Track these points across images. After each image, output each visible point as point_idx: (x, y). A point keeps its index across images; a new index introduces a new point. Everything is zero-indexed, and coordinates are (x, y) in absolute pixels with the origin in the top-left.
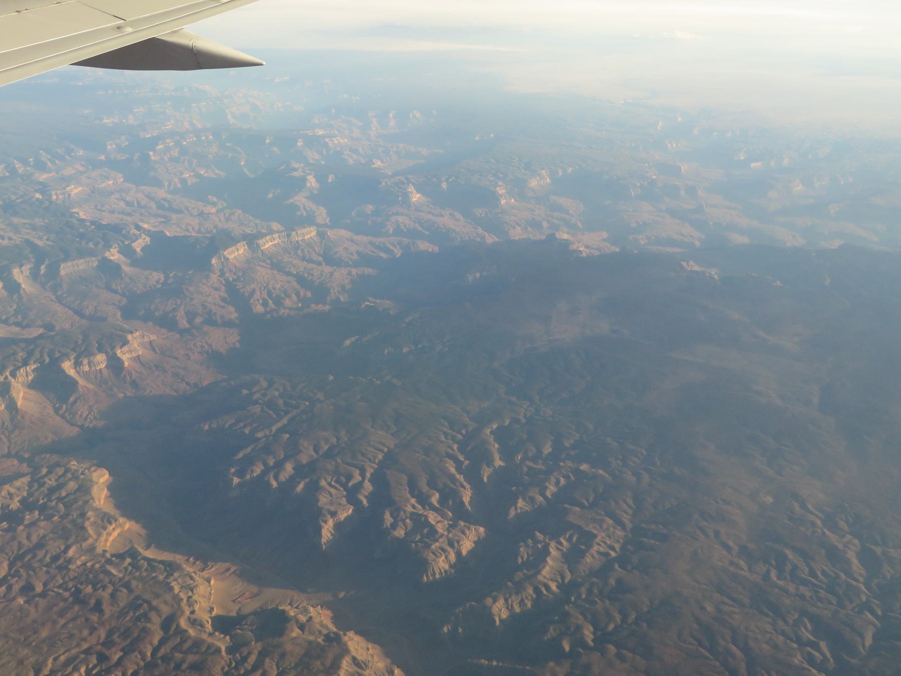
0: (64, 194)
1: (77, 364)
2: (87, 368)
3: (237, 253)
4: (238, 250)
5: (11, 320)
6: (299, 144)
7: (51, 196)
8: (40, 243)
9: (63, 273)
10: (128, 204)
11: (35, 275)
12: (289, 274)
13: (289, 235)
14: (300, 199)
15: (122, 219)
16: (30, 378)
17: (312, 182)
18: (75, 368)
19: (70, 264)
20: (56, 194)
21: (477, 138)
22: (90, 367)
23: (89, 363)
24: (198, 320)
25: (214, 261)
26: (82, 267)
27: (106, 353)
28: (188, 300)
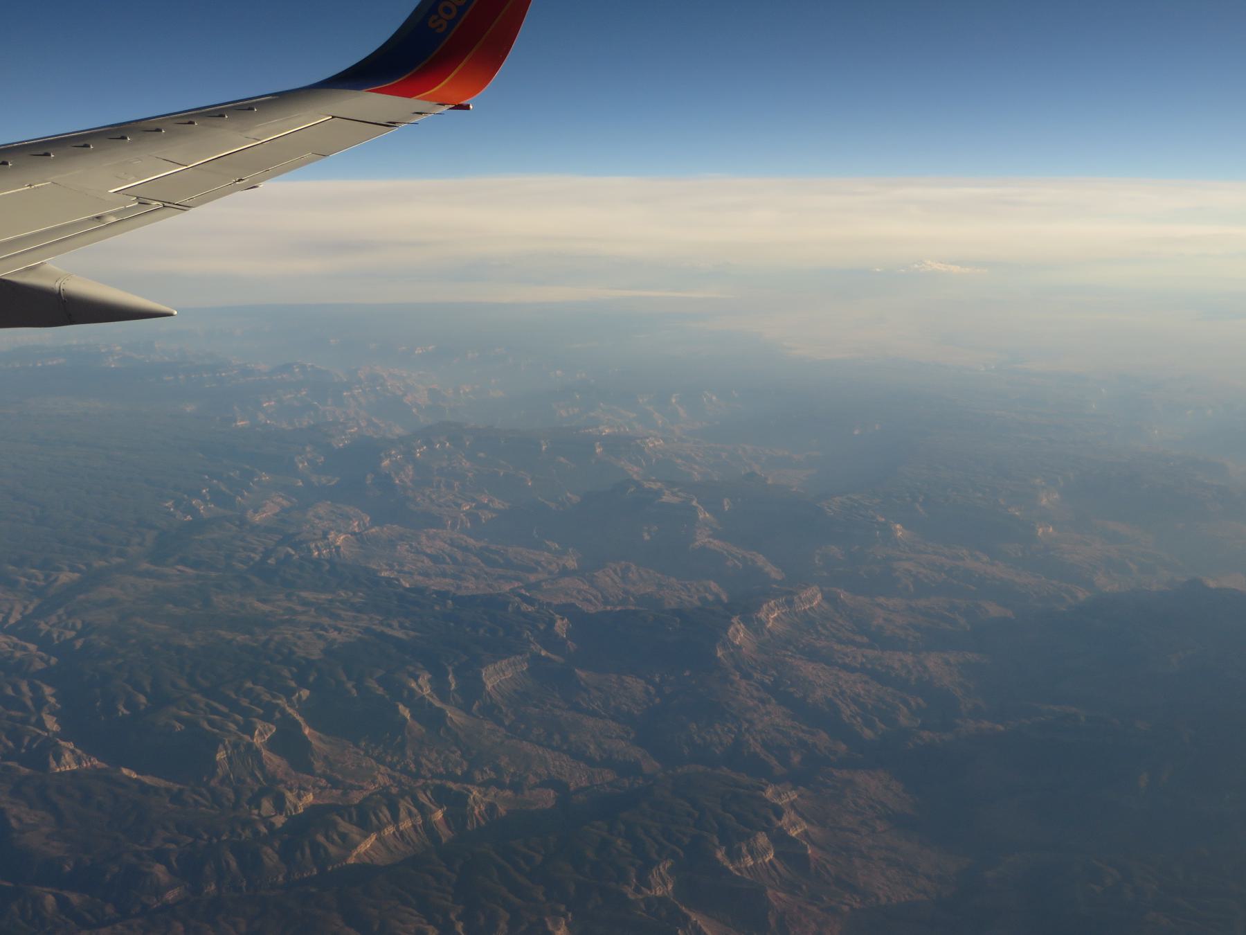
0: (328, 546)
1: (734, 855)
2: (750, 862)
3: (739, 634)
4: (738, 631)
5: (478, 776)
6: (598, 450)
7: (310, 550)
8: (399, 634)
9: (489, 686)
10: (435, 559)
11: (441, 690)
12: (845, 667)
13: (790, 603)
14: (702, 539)
15: (459, 587)
16: (670, 887)
17: (703, 515)
18: (732, 863)
19: (491, 668)
20: (317, 548)
21: (856, 432)
22: (753, 858)
23: (751, 852)
24: (796, 759)
25: (719, 654)
26: (509, 674)
27: (765, 830)
28: (746, 725)
